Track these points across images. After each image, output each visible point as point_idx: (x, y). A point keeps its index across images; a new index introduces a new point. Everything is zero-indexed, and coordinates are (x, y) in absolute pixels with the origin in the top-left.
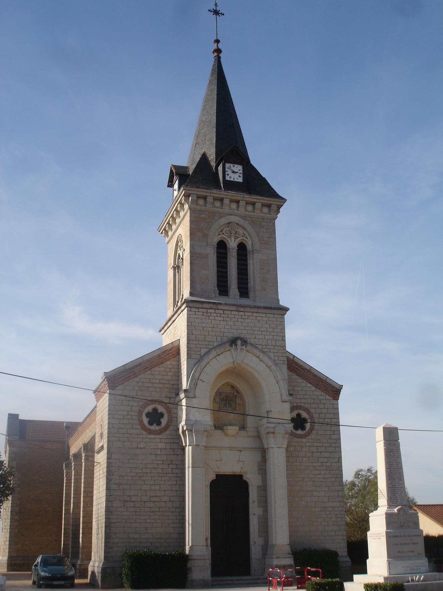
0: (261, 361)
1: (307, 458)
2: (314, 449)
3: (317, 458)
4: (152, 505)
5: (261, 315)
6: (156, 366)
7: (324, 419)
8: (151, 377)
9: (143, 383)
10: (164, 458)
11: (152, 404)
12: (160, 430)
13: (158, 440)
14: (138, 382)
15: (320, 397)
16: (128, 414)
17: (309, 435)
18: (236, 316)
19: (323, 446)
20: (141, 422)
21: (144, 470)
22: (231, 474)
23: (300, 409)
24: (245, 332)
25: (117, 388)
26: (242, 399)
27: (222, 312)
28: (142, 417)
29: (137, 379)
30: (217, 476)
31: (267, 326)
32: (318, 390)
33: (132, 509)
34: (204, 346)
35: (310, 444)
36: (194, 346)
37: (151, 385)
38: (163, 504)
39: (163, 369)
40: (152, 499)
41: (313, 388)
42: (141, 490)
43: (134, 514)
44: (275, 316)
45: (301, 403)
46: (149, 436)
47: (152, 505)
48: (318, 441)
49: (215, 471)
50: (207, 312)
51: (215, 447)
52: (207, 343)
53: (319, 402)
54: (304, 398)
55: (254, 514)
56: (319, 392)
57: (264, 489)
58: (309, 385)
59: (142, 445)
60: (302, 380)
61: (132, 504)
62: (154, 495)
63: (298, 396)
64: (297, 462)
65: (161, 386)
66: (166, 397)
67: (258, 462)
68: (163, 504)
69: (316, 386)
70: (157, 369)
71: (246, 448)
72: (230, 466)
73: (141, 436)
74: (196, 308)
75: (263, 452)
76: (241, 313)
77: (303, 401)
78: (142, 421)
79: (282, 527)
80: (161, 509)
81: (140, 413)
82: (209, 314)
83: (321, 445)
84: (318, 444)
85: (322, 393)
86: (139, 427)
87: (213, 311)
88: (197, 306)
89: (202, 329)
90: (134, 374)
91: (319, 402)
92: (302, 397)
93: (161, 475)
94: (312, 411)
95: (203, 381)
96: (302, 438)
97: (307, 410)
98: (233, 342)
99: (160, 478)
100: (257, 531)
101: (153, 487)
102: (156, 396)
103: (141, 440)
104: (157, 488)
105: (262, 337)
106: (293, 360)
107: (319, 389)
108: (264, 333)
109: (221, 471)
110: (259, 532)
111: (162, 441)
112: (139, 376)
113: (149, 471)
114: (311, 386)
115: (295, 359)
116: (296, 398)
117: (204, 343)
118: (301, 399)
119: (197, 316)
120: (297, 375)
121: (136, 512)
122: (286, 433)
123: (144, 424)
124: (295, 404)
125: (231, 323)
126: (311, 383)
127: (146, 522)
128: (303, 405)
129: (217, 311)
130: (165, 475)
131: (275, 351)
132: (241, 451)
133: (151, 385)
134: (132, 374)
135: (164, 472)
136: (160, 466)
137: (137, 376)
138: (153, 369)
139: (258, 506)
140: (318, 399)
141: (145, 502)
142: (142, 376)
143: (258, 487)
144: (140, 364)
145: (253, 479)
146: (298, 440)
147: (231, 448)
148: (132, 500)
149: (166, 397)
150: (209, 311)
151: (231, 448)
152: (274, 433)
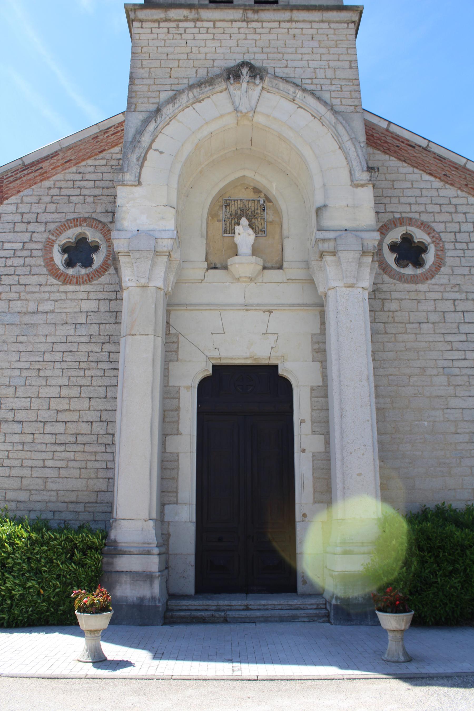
0: (300, 107)
1: (431, 326)
2: (448, 306)
3: (455, 325)
4: (60, 428)
5: (300, 25)
6: (89, 158)
7: (467, 243)
8: (79, 177)
9: (60, 188)
10: (94, 330)
11: (75, 226)
12: (88, 275)
13: (85, 296)
14: (50, 188)
15: (454, 201)
16: (23, 249)
17: (433, 276)
18: (242, 30)
19: (467, 299)
20: (49, 263)
21: (48, 357)
22: (249, 362)
23: (410, 225)
24: (264, 56)
25: (6, 202)
26: (278, 212)
27: (211, 24)
28: (51, 252)
29: (47, 183)
30: (214, 367)
31: (315, 44)
32: (447, 186)
33: (16, 438)
34: (168, 87)
35: (438, 296)
36: (146, 88)
37: (77, 192)
38: (85, 428)
39: (104, 162)
40: (62, 417)
41: (437, 184)
42: (38, 397)
43: (20, 447)
44: (333, 25)
45: (411, 212)
46: (63, 288)
47: (60, 428)
48: (456, 289)
49: (208, 354)
50: (178, 27)
51: (208, 305)
52: (176, 81)
53: (453, 210)
54: (416, 203)
55: (304, 451)
56: (451, 191)
57: (322, 392)
58: (427, 177)
59: (47, 306)
60: (410, 169)
61: (17, 428)
62: (67, 407)
63: (402, 200)
64: (406, 333)
65: (97, 192)
66: (107, 212)
67: (313, 335)
68: (85, 428)
69: (445, 178)
70: (90, 162)
71: (283, 305)
72: (244, 346)
73: (48, 289)
74: (154, 21)
75: (320, 306)
76: (254, 25)
77: (414, 208)
78: (52, 259)
79: (359, 475)
80: (80, 438)
81: (49, 245)
82: (182, 31)
83: (463, 296)
84: (457, 296)
85: (459, 192)
86: (44, 271)
87: (191, 24)
88: (155, 17)
89: (164, 56)
90: (41, 175)
91: (453, 210)
92: (412, 200)
93: (83, 365)
94: (439, 227)
95: (161, 153)
96: (416, 283)
97: (424, 226)
98: (233, 74)
99: (82, 373)
100: (309, 489)
101: (65, 392)
102: (84, 211)
103: (47, 295)
104: (75, 392)
105: (304, 63)
106: (387, 130)
107: (452, 184)
108: (306, 57)
109: (224, 354)
110: (315, 491)
111: (92, 296)
112: (54, 178)
113: (58, 357)
114: (432, 179)
115: (393, 128)
116: (399, 203)
117: (169, 81)
118: (410, 204)
119: (155, 36)
120: (400, 159)
121: (23, 444)
122: (364, 253)
123: (55, 264)
124: (397, 216)
125: (232, 43)
126: (431, 174)
127: (44, 467)
128: (416, 216)
129: (199, 24)
130: (94, 365)
131: (333, 88)
132: (271, 312)
133: (77, 192)
134: (37, 174)
135: (91, 359)
136: (83, 348)
137: (48, 178)
138: (83, 163)
139: (314, 432)
140: (450, 203)
141: (45, 422)
142: (59, 177)
143: (312, 389)
144: (56, 154)
145: (299, 372)
146: (408, 286)
147: (246, 307)
148: (17, 419)
149: (107, 212)
150: (182, 25)
151: (246, 307)
152: (334, 253)
